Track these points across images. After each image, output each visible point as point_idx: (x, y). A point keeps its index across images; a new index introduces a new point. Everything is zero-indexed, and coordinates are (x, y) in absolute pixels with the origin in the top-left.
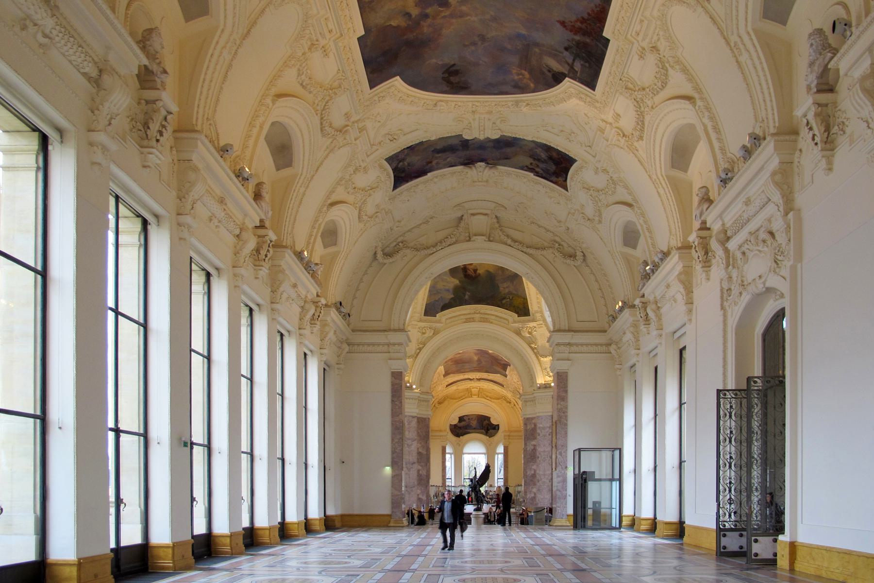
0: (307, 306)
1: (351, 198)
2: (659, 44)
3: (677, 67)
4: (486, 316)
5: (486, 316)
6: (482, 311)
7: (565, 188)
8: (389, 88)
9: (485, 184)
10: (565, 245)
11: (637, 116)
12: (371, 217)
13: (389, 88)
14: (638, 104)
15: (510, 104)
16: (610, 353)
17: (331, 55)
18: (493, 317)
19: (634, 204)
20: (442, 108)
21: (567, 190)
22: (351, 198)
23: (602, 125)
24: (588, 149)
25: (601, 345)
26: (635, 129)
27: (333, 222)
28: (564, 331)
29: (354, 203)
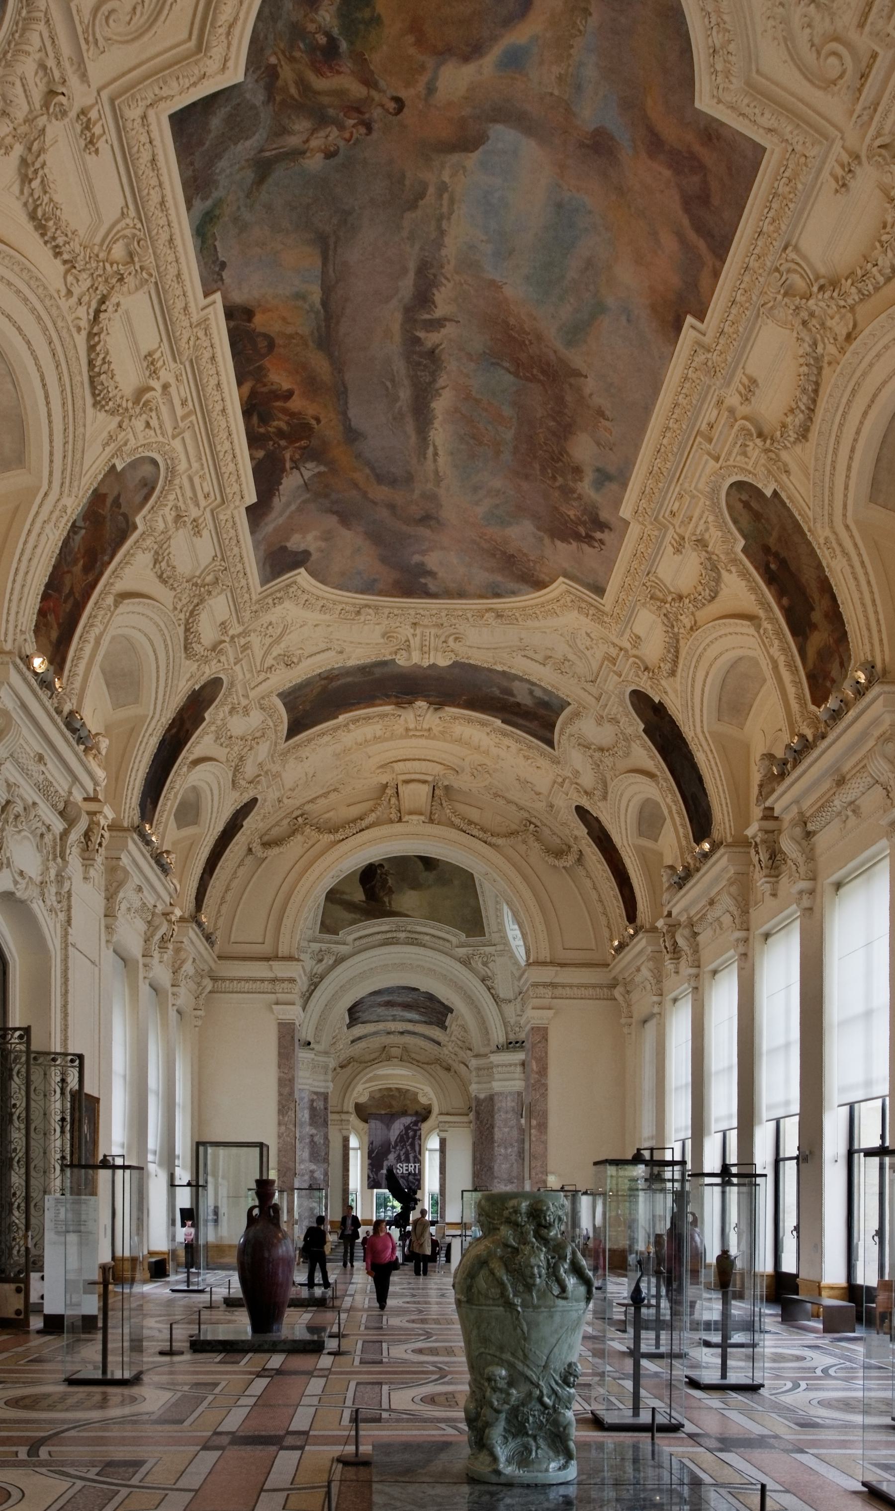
1: (220, 753)
3: (733, 569)
7: (550, 743)
8: (289, 586)
10: (547, 832)
11: (667, 639)
12: (250, 783)
13: (289, 586)
14: (670, 621)
16: (615, 999)
19: (658, 773)
20: (369, 617)
21: (553, 747)
22: (220, 753)
23: (613, 652)
24: (589, 686)
26: (663, 660)
27: (194, 788)
28: (544, 964)
29: (228, 761)
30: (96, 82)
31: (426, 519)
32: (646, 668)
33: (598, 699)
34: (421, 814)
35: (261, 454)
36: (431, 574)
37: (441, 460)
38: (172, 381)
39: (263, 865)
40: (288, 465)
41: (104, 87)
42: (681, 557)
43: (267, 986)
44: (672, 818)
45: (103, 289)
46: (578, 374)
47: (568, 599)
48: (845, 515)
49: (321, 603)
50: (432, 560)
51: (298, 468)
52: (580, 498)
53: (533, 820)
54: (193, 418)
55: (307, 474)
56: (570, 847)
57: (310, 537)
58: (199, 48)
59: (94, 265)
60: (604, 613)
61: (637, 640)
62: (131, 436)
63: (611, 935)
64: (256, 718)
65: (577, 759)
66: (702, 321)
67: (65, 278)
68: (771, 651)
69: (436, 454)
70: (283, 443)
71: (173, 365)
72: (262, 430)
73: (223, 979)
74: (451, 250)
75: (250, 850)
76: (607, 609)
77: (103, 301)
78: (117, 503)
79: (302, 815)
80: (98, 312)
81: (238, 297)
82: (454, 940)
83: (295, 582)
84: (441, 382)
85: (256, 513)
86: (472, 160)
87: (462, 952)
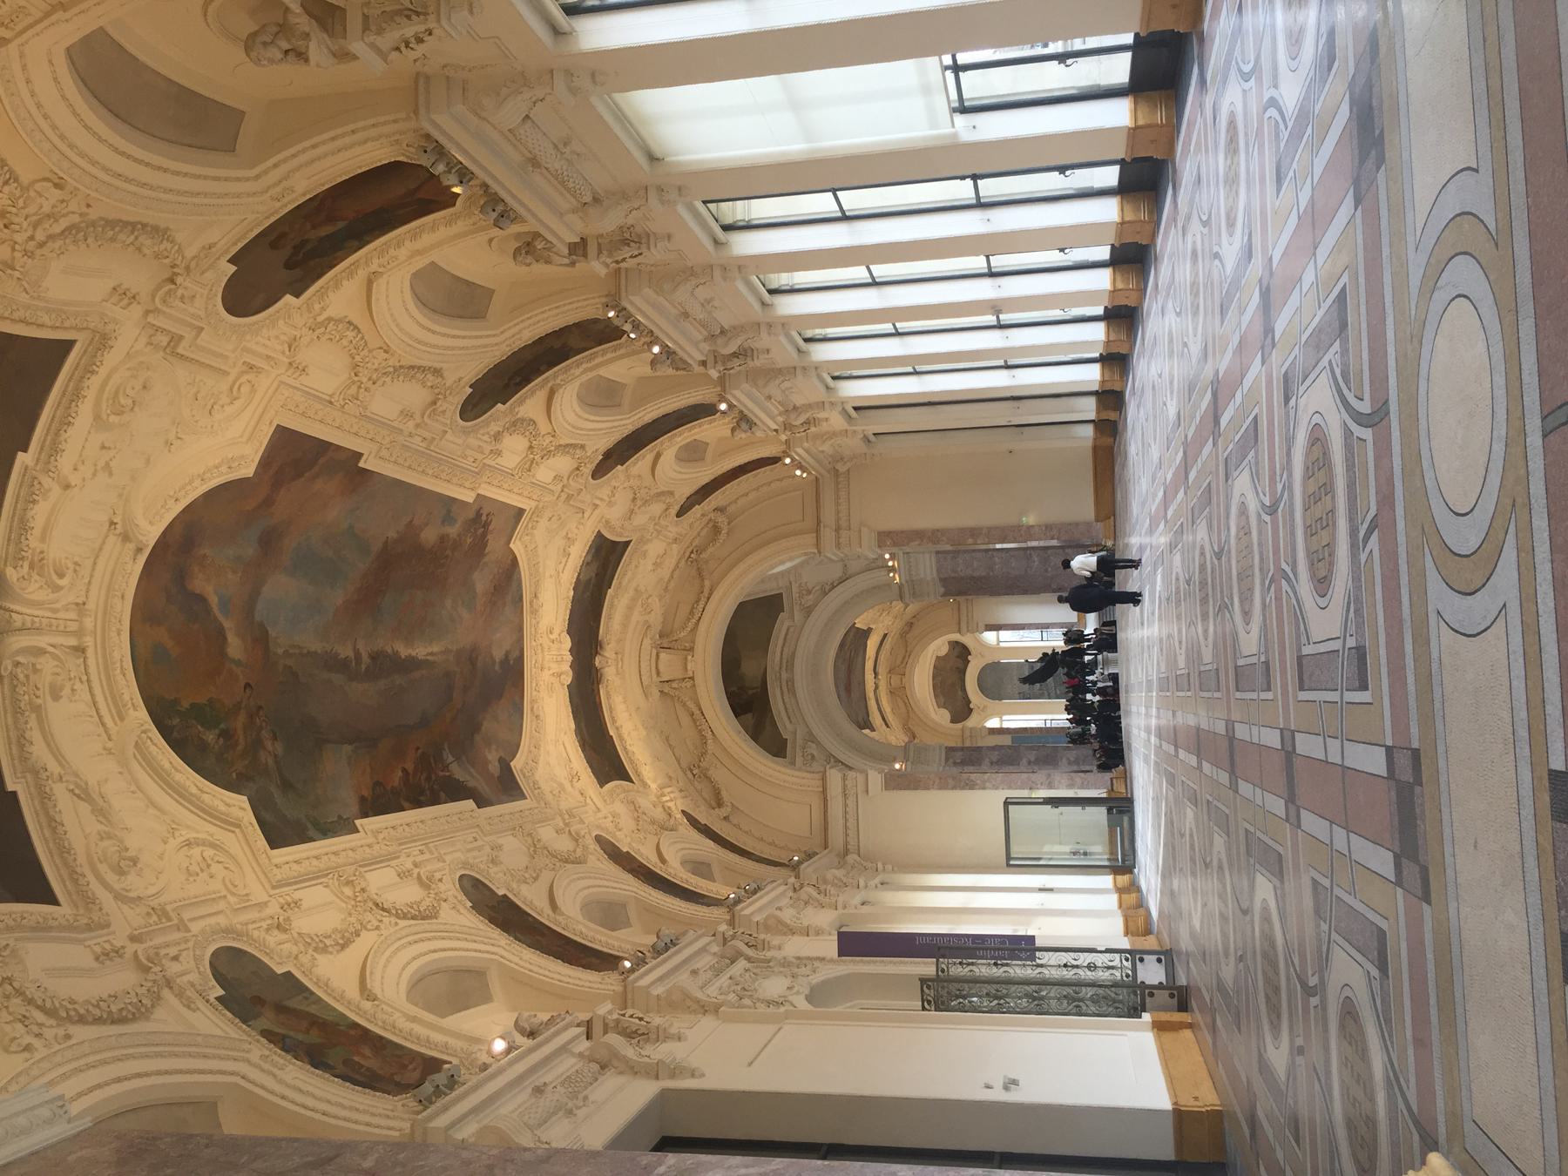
0: (804, 897)
2: (492, 433)
4: (785, 661)
5: (785, 661)
6: (777, 669)
7: (627, 543)
9: (620, 656)
10: (696, 542)
14: (547, 454)
15: (534, 621)
16: (848, 470)
17: (500, 841)
18: (786, 650)
23: (564, 496)
24: (586, 515)
25: (837, 483)
28: (818, 539)
29: (656, 834)
30: (265, 898)
31: (472, 661)
32: (577, 469)
33: (596, 506)
34: (686, 659)
35: (442, 795)
36: (507, 656)
37: (435, 648)
38: (411, 859)
39: (737, 805)
40: (447, 774)
41: (267, 893)
42: (504, 451)
43: (851, 802)
44: (695, 434)
45: (371, 905)
46: (386, 542)
47: (526, 538)
48: (494, 336)
49: (533, 749)
50: (498, 655)
51: (447, 766)
52: (459, 535)
53: (687, 554)
54: (431, 845)
55: (451, 759)
56: (710, 520)
57: (490, 757)
58: (239, 826)
59: (359, 909)
60: (537, 507)
61: (557, 478)
62: (450, 893)
63: (789, 477)
64: (619, 807)
65: (640, 519)
66: (362, 454)
67: (369, 930)
68: (577, 373)
69: (432, 654)
70: (434, 778)
71: (402, 859)
72: (428, 792)
73: (846, 843)
74: (316, 646)
75: (726, 818)
76: (533, 504)
77: (377, 905)
78: (493, 908)
79: (691, 771)
80: (383, 909)
81: (355, 808)
82: (787, 624)
83: (521, 770)
84: (390, 651)
85: (482, 802)
86: (272, 633)
87: (798, 616)
